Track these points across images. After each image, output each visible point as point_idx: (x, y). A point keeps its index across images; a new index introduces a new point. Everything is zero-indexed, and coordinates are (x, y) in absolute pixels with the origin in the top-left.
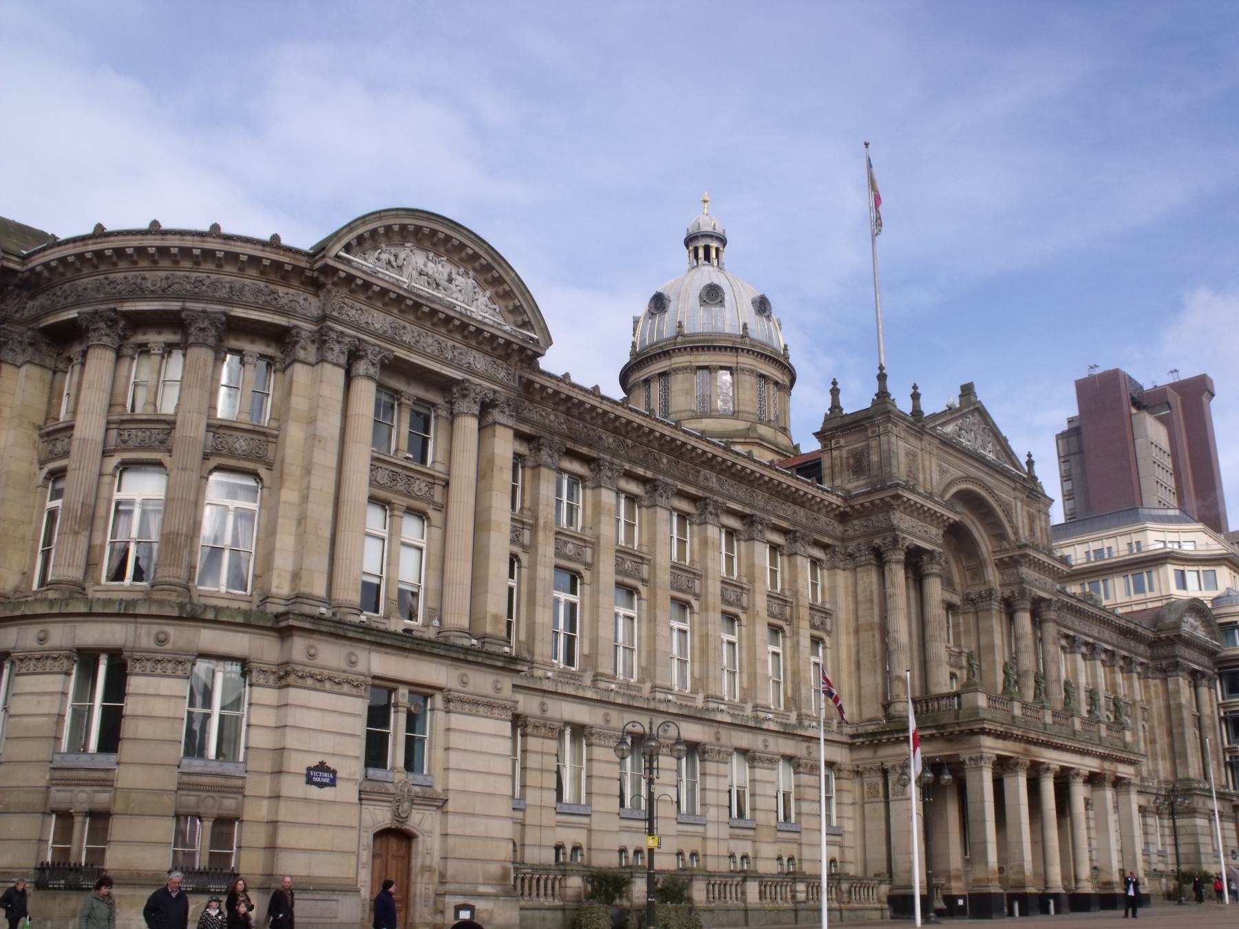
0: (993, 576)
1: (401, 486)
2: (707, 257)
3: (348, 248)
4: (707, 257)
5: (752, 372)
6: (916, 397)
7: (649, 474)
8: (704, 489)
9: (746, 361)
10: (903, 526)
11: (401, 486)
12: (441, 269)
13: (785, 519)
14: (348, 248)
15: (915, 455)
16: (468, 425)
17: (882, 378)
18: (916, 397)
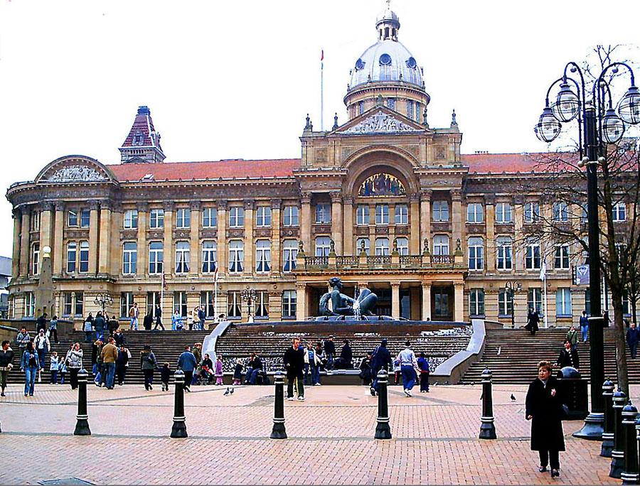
0: (412, 185)
1: (78, 235)
2: (387, 35)
3: (43, 178)
4: (387, 35)
5: (371, 99)
6: (336, 118)
7: (188, 200)
8: (214, 198)
9: (369, 95)
10: (306, 187)
11: (78, 235)
12: (75, 170)
13: (265, 196)
14: (43, 178)
15: (324, 150)
16: (94, 213)
17: (308, 119)
18: (336, 118)
